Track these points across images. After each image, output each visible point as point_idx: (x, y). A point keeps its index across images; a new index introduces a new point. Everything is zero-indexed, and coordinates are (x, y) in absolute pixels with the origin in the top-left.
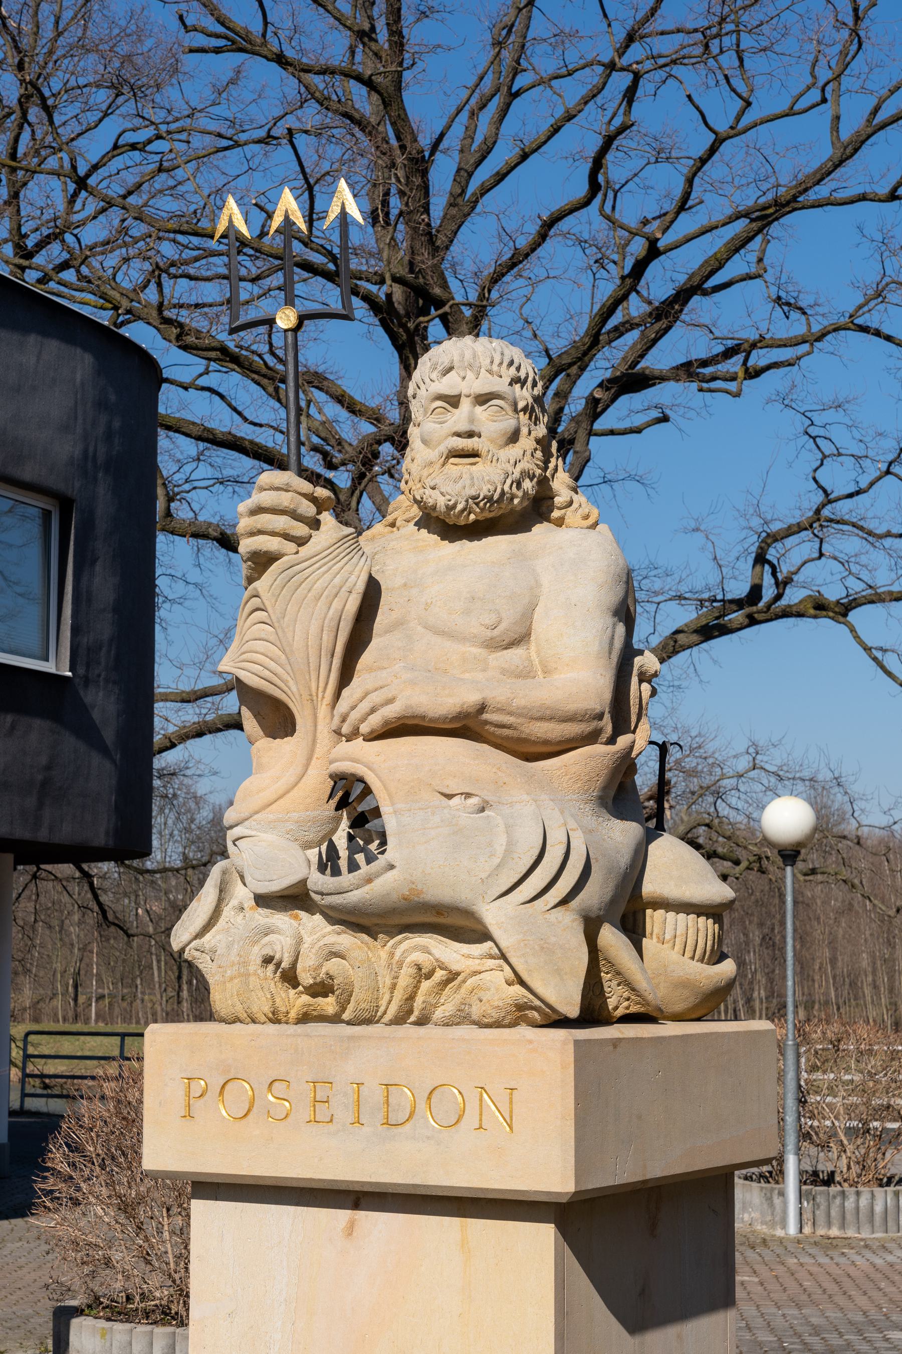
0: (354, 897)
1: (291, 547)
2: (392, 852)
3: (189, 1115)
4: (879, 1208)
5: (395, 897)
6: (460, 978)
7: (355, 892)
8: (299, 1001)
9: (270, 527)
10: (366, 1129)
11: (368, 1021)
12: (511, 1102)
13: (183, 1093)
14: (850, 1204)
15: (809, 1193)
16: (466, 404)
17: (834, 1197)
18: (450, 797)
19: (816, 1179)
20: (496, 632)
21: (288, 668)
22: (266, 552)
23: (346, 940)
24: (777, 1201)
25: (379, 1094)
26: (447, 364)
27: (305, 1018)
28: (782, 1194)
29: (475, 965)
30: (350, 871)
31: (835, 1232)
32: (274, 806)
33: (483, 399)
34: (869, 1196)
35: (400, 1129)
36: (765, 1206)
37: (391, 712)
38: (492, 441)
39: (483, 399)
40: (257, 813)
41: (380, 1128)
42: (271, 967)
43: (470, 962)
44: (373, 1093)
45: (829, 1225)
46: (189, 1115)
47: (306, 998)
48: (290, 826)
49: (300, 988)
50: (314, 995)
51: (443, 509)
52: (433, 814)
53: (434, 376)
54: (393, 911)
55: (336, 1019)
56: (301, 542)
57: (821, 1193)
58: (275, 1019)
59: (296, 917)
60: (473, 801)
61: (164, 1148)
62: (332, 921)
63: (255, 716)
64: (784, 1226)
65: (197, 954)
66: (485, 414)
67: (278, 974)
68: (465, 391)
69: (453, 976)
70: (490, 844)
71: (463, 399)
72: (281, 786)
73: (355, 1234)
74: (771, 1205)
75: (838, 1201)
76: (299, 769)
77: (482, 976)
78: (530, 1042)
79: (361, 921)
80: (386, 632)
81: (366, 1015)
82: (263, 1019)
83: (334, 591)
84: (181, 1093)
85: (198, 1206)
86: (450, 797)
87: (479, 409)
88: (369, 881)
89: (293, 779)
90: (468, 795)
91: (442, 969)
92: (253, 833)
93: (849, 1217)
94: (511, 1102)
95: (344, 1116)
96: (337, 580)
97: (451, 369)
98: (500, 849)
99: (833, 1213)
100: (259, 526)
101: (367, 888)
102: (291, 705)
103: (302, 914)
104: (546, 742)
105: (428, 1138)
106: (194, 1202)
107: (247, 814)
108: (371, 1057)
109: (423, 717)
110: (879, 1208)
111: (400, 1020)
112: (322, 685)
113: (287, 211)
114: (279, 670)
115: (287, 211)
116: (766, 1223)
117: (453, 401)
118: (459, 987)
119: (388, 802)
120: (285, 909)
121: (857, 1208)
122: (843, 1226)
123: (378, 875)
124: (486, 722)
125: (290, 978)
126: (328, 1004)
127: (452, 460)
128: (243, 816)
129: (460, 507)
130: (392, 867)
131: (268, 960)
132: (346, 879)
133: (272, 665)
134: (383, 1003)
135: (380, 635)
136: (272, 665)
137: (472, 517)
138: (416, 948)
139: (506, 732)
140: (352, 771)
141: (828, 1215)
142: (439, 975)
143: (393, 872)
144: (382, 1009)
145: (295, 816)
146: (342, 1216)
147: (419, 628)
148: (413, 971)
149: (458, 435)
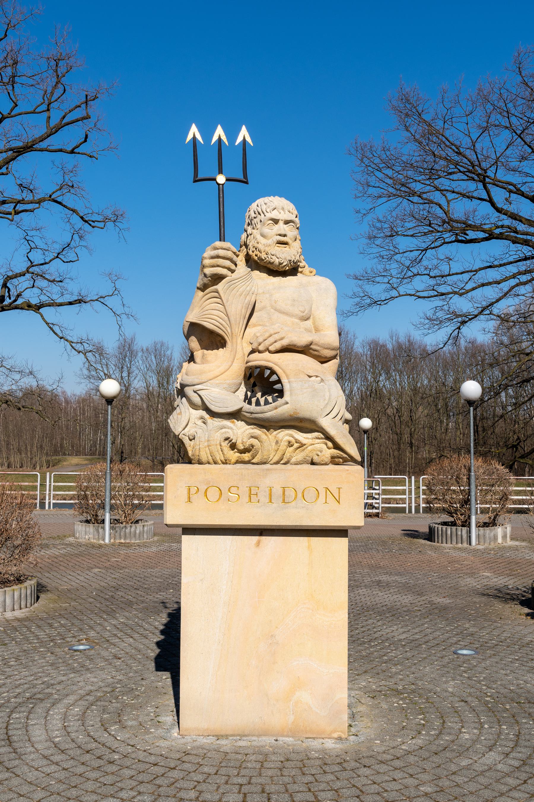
0: (268, 415)
1: (229, 273)
2: (287, 397)
3: (189, 500)
4: (138, 532)
5: (286, 415)
6: (305, 447)
7: (269, 413)
8: (234, 455)
9: (223, 265)
10: (274, 505)
11: (265, 463)
12: (339, 493)
13: (187, 492)
14: (128, 531)
15: (113, 527)
16: (281, 223)
17: (123, 528)
18: (310, 377)
19: (115, 522)
20: (304, 314)
21: (228, 322)
22: (221, 275)
23: (257, 431)
24: (101, 530)
25: (280, 491)
26: (274, 207)
27: (237, 462)
28: (103, 528)
29: (310, 441)
30: (265, 404)
31: (122, 541)
32: (219, 377)
33: (287, 222)
34: (135, 527)
35: (290, 504)
36: (95, 533)
37: (285, 342)
38: (291, 239)
39: (287, 222)
40: (210, 380)
41: (281, 504)
42: (227, 442)
43: (308, 440)
44: (277, 491)
45: (120, 538)
46: (189, 500)
47: (238, 454)
48: (225, 386)
49: (236, 450)
50: (241, 453)
51: (278, 264)
52: (305, 383)
53: (268, 210)
54: (284, 420)
55: (249, 462)
56: (233, 271)
57: (118, 527)
58: (225, 462)
59: (233, 422)
60: (319, 379)
61: (175, 513)
62: (248, 424)
63: (198, 341)
64: (104, 540)
65: (184, 436)
66: (287, 228)
67: (229, 444)
68: (281, 218)
69: (302, 445)
70: (324, 396)
71: (280, 221)
72: (222, 369)
73: (260, 545)
74: (98, 532)
75: (124, 530)
76: (230, 363)
77: (315, 445)
78: (348, 470)
79: (262, 423)
80: (260, 310)
81: (265, 461)
82: (220, 462)
83: (248, 292)
84: (186, 492)
85: (186, 539)
86: (310, 377)
87: (285, 226)
88: (276, 408)
89: (227, 367)
90: (317, 376)
91: (296, 442)
92: (208, 388)
93: (127, 535)
94: (339, 493)
95: (264, 499)
96: (248, 288)
97: (275, 208)
98: (327, 398)
99: (122, 534)
100: (219, 264)
101: (274, 411)
102: (226, 337)
103: (235, 421)
104: (326, 357)
105: (303, 507)
106: (183, 536)
107: (206, 380)
108: (275, 478)
109: (295, 346)
110: (138, 532)
111: (277, 463)
112: (240, 330)
113: (220, 135)
114: (224, 323)
115: (220, 135)
116: (96, 539)
117: (276, 221)
118: (304, 450)
119: (286, 378)
120: (229, 419)
121: (130, 532)
122: (125, 539)
123: (280, 406)
124: (311, 349)
125: (233, 446)
126: (246, 456)
127: (277, 245)
128: (203, 381)
129: (285, 264)
130: (287, 403)
131: (226, 439)
132: (263, 408)
133: (221, 321)
134: (271, 456)
135: (257, 312)
136: (221, 321)
137: (287, 268)
138: (287, 435)
139: (316, 353)
140: (267, 365)
141: (120, 535)
142: (296, 445)
143: (288, 405)
144: (271, 458)
145: (228, 382)
146: (255, 539)
147: (272, 310)
148: (287, 443)
149: (280, 235)
